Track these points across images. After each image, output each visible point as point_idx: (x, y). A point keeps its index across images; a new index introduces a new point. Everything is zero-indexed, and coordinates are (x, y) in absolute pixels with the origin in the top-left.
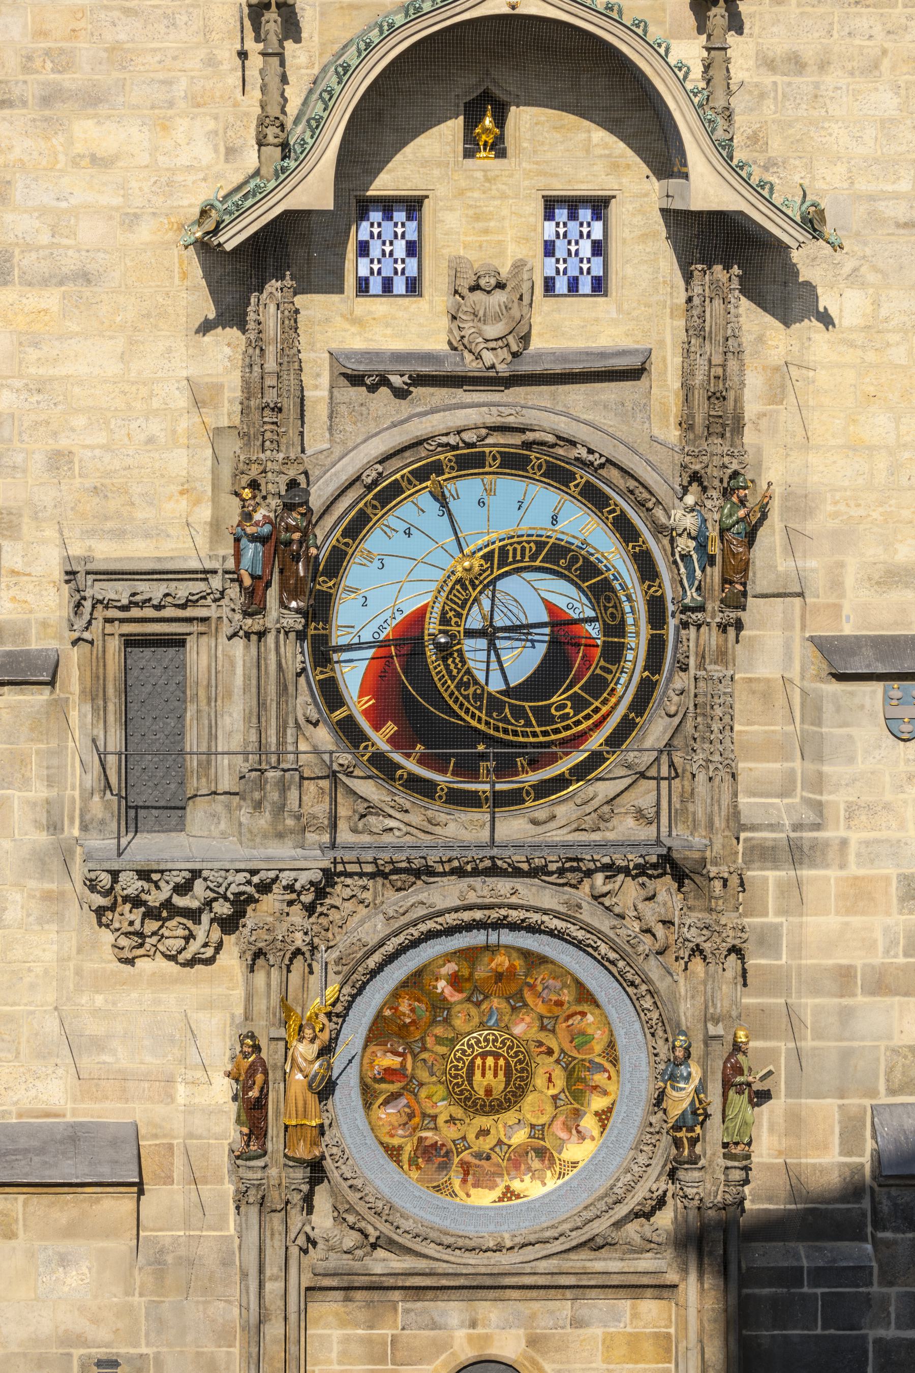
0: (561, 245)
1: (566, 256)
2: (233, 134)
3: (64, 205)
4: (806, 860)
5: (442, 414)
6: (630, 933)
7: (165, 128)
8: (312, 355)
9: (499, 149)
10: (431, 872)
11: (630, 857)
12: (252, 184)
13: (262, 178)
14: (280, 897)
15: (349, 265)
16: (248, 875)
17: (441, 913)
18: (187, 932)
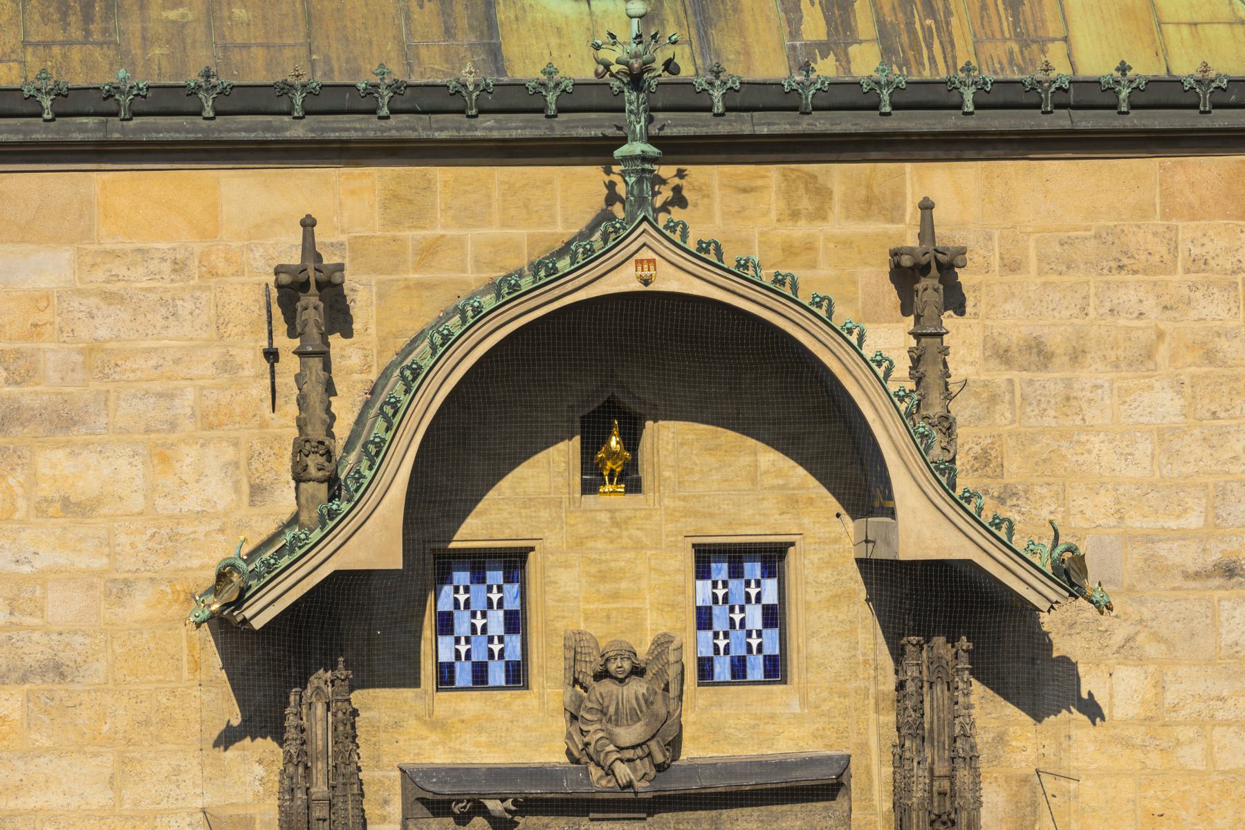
0: (719, 612)
1: (727, 628)
2: (259, 466)
3: (26, 569)
7: (165, 460)
8: (377, 774)
9: (631, 481)
12: (288, 536)
13: (301, 527)
15: (426, 647)
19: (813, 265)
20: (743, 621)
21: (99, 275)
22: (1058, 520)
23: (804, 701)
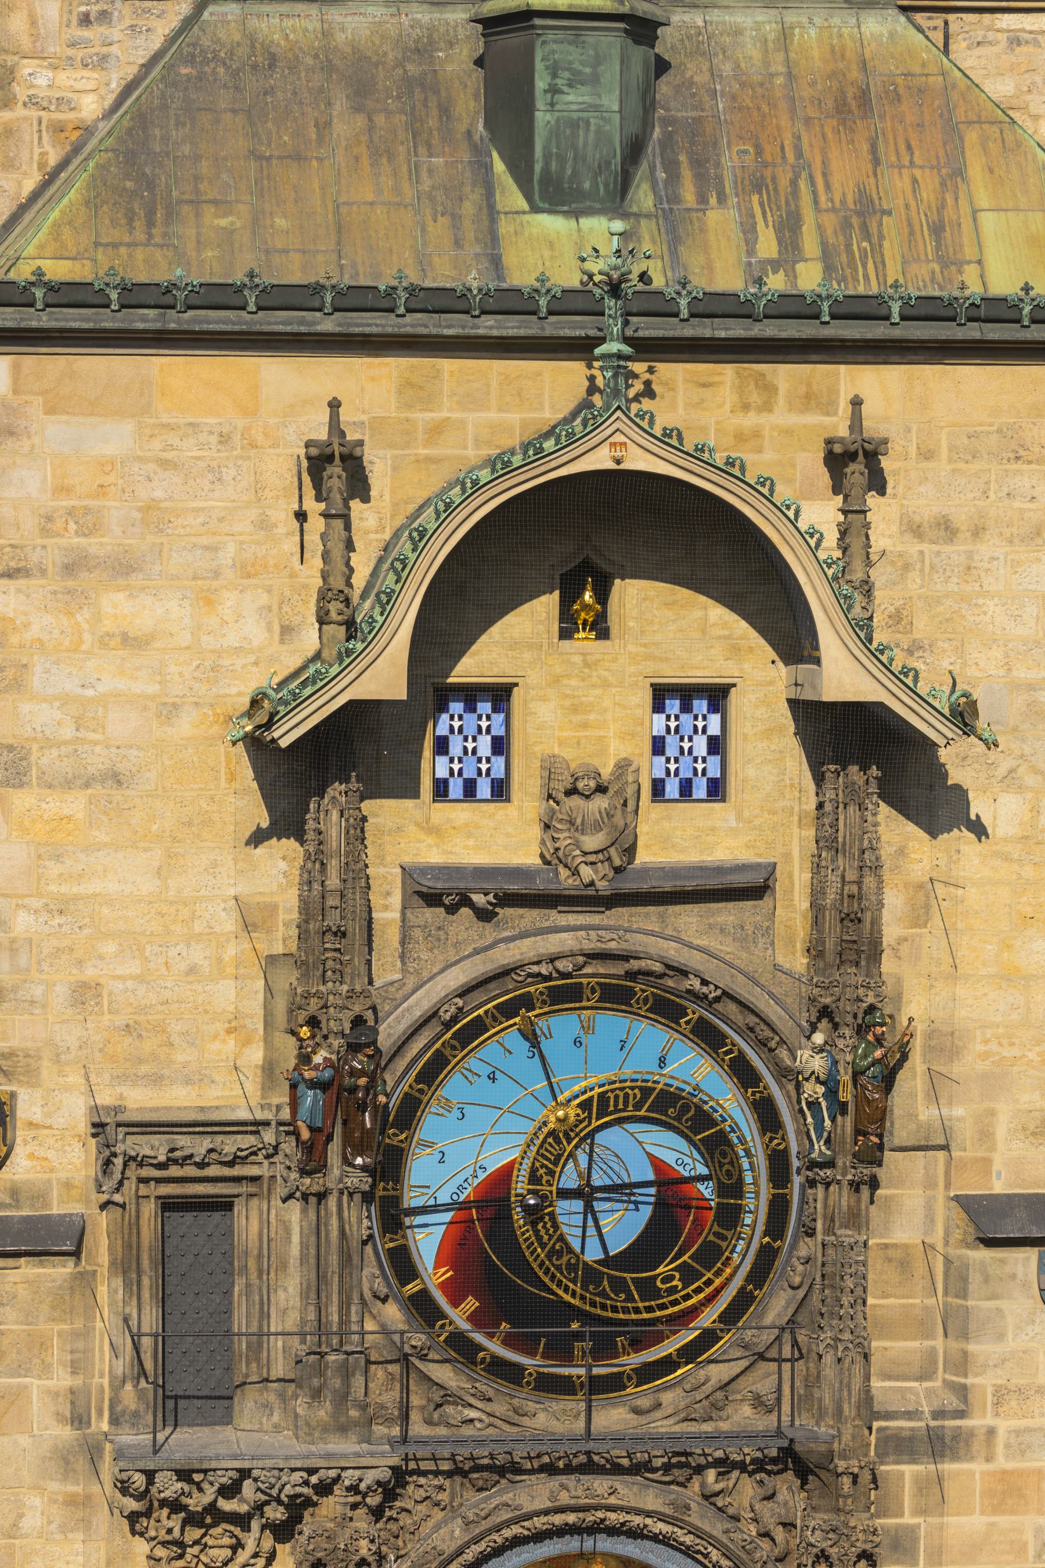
0: (671, 741)
1: (677, 755)
2: (289, 610)
3: (90, 693)
4: (948, 1452)
5: (533, 939)
6: (746, 1537)
7: (209, 603)
8: (382, 870)
9: (601, 629)
10: (518, 1470)
11: (746, 1451)
12: (311, 670)
13: (323, 662)
14: (342, 1500)
15: (425, 765)
16: (305, 1475)
17: (528, 1517)
18: (234, 1541)
19: (760, 450)
20: (690, 749)
21: (156, 445)
22: (956, 669)
23: (739, 817)
